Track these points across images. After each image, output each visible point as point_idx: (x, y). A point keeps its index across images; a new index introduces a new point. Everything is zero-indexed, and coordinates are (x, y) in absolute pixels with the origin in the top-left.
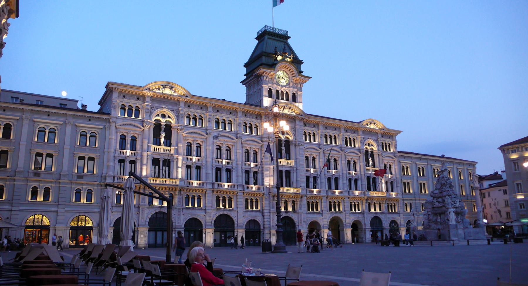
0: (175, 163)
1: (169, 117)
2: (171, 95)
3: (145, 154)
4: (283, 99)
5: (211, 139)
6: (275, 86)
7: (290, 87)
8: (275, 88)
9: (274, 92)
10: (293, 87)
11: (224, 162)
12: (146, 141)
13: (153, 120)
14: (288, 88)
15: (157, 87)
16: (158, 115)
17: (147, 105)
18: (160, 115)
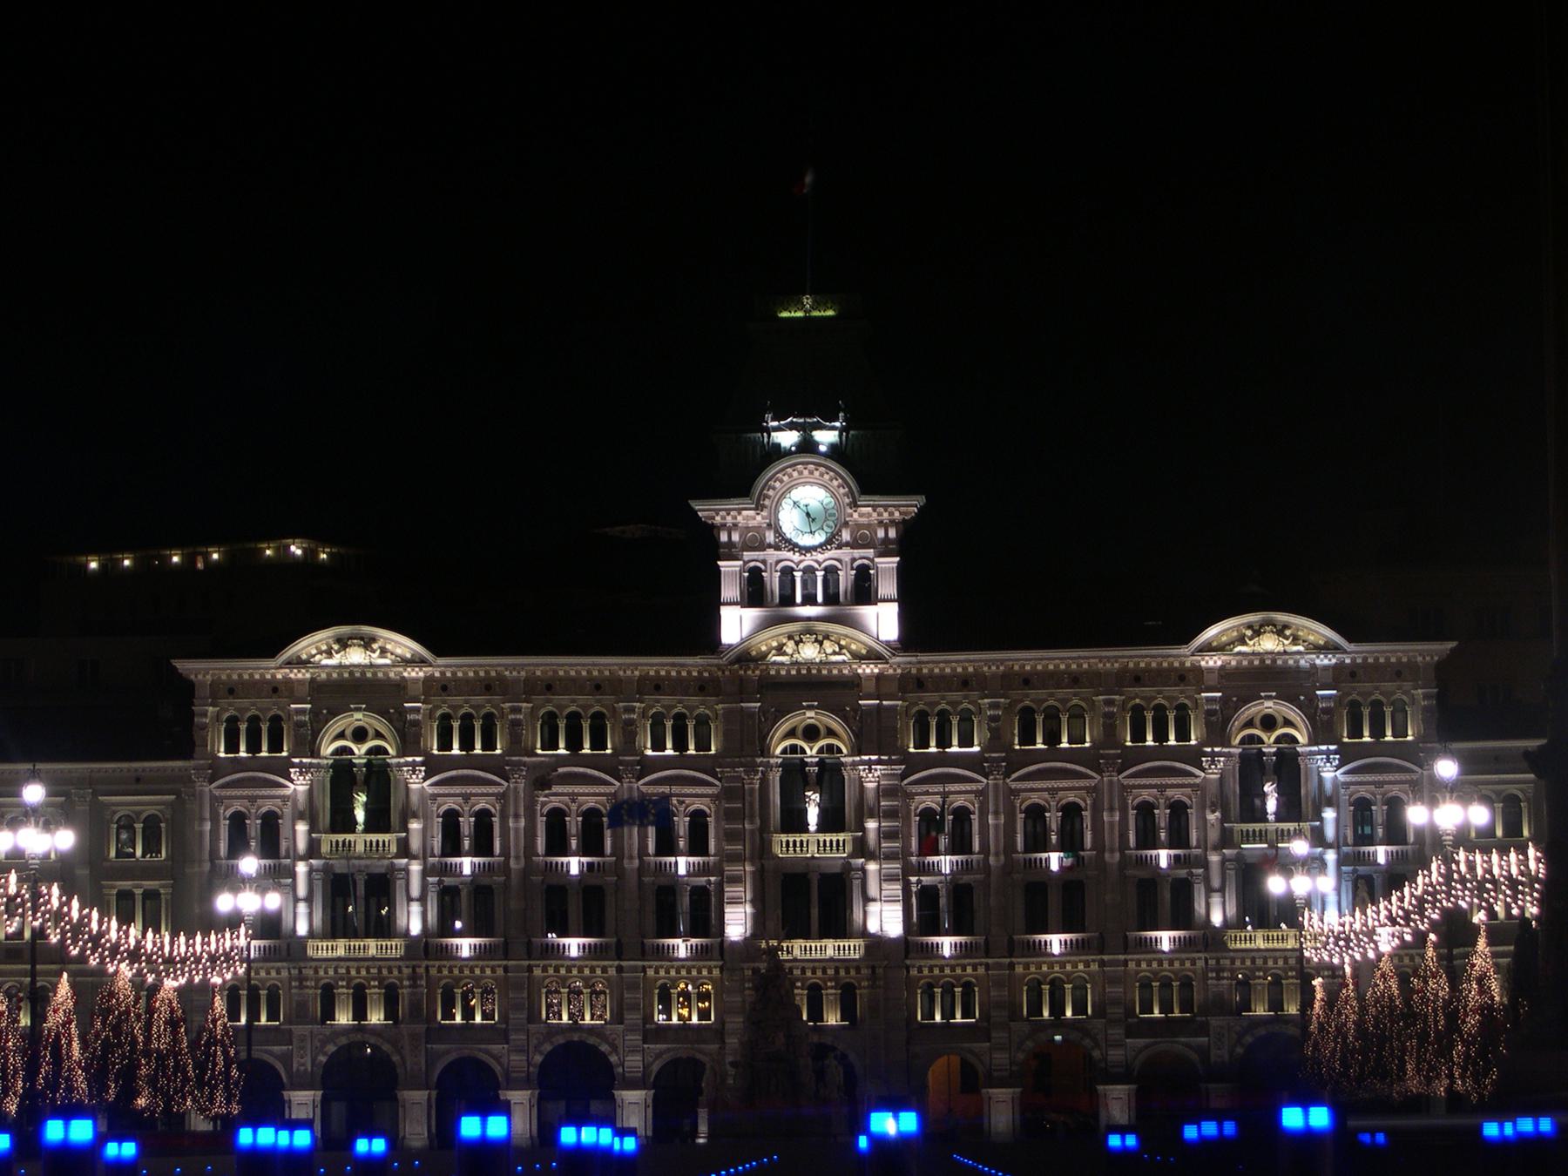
0: (400, 884)
1: (379, 735)
2: (372, 665)
4: (809, 600)
6: (771, 555)
7: (839, 547)
9: (773, 581)
10: (854, 544)
11: (1164, 857)
13: (778, 751)
14: (834, 553)
15: (324, 648)
16: (341, 736)
17: (1209, 700)
18: (1257, 721)
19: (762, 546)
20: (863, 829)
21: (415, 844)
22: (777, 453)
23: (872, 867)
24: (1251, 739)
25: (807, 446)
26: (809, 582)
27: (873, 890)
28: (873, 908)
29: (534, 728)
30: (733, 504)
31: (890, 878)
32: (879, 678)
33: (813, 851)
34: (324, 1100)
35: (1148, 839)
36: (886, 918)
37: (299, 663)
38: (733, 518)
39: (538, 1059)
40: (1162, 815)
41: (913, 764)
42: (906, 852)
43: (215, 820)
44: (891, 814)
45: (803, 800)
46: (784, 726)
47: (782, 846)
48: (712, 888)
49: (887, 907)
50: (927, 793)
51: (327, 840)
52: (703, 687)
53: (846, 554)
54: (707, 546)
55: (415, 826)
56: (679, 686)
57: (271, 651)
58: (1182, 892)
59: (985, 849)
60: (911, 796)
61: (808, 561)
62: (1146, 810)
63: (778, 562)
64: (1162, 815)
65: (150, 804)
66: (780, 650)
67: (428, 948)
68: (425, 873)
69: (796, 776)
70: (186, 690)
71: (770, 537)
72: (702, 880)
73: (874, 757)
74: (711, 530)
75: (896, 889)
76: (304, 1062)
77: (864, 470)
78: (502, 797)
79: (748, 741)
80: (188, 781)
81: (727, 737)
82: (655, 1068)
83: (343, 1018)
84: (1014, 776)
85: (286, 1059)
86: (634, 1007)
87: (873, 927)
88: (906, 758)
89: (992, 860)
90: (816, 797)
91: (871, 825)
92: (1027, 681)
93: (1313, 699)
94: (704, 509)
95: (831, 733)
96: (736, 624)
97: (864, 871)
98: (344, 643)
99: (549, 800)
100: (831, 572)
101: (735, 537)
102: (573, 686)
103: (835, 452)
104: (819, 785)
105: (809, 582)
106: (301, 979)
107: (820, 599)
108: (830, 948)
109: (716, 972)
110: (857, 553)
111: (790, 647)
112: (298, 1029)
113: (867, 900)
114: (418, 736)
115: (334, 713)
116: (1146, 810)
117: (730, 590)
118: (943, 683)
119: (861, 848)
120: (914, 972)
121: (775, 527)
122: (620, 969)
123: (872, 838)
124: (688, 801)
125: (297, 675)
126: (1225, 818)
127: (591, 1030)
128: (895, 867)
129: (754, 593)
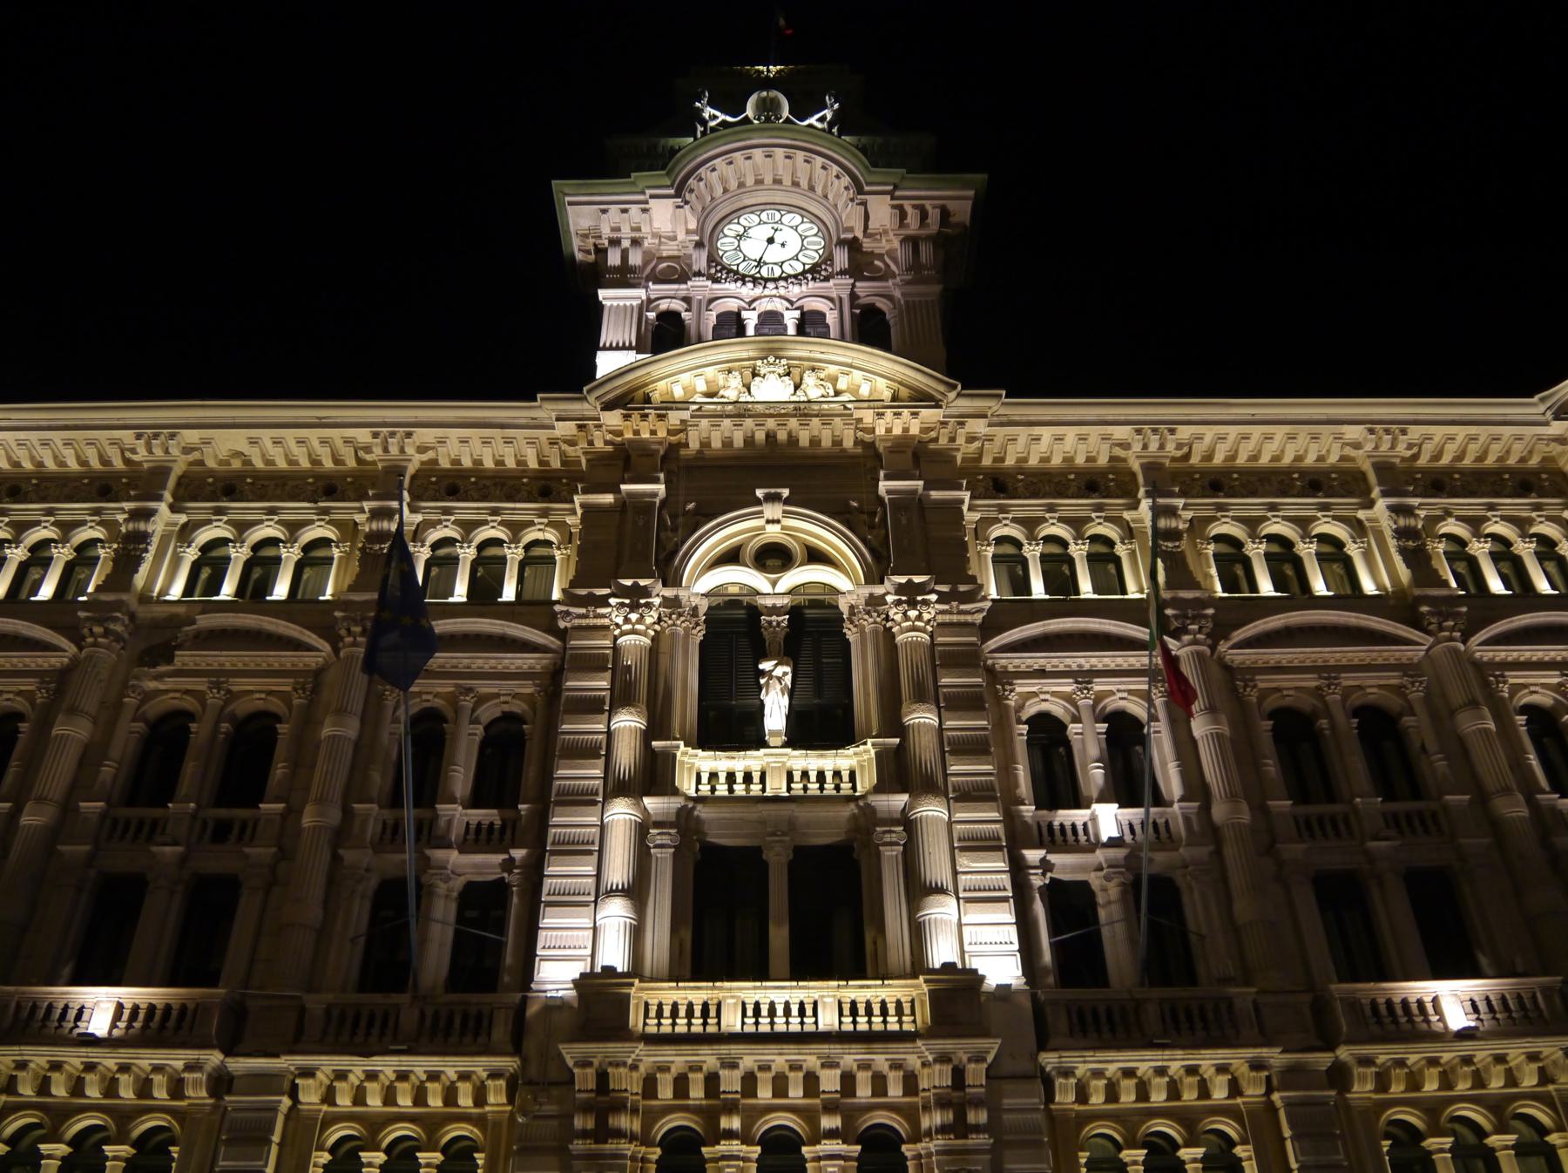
6: (700, 287)
20: (900, 730)
23: (932, 811)
27: (936, 867)
28: (941, 911)
29: (176, 562)
31: (978, 844)
36: (984, 941)
42: (1009, 805)
45: (754, 683)
48: (513, 878)
49: (974, 914)
50: (1042, 673)
59: (1196, 787)
63: (711, 301)
69: (734, 634)
71: (700, 261)
73: (917, 579)
75: (992, 869)
79: (632, 548)
84: (1240, 634)
89: (1219, 812)
90: (783, 671)
91: (922, 718)
92: (1219, 483)
97: (908, 823)
99: (166, 688)
101: (635, 259)
104: (789, 651)
108: (828, 1001)
109: (497, 1097)
110: (863, 288)
113: (919, 890)
119: (898, 771)
120: (1065, 1097)
122: (221, 1083)
123: (925, 749)
124: (485, 687)
128: (985, 818)
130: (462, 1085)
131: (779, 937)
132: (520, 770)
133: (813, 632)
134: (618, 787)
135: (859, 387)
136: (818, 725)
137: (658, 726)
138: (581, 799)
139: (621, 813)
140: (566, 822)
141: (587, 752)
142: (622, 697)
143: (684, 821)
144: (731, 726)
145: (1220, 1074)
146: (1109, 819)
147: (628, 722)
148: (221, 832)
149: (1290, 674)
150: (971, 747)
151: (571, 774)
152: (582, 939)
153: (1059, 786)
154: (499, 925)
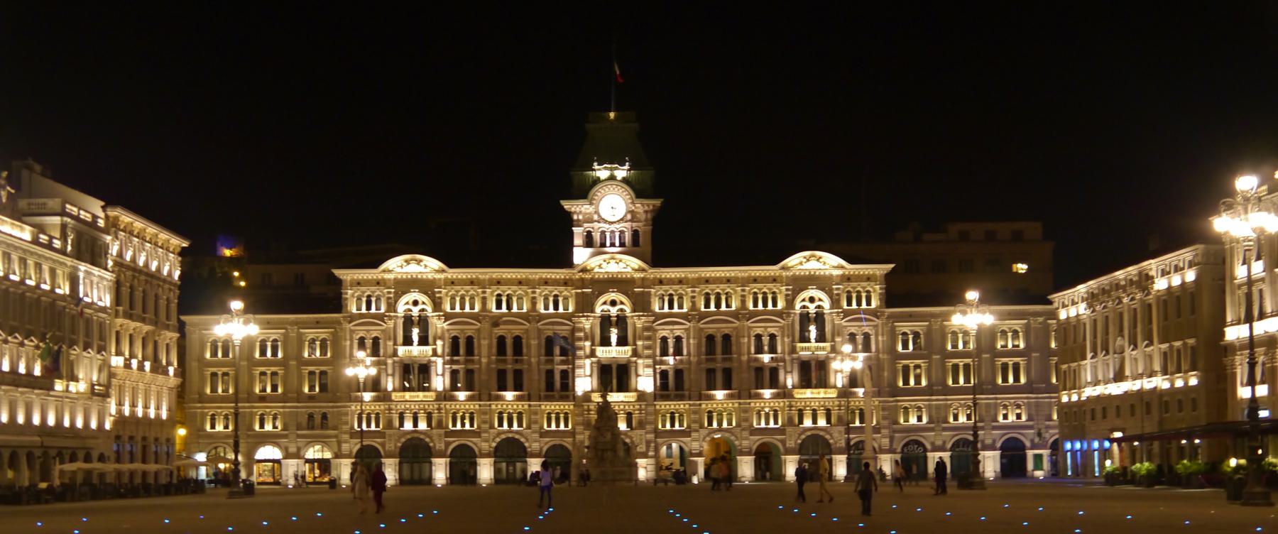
0: (433, 368)
3: (390, 361)
4: (613, 245)
5: (486, 325)
6: (596, 225)
8: (597, 228)
9: (597, 237)
12: (390, 343)
19: (592, 221)
21: (439, 351)
22: (597, 181)
23: (640, 361)
24: (804, 307)
25: (612, 178)
26: (612, 238)
27: (640, 371)
30: (581, 202)
31: (648, 366)
32: (643, 279)
33: (614, 355)
34: (400, 463)
35: (759, 350)
37: (390, 271)
38: (578, 208)
39: (494, 445)
40: (766, 340)
41: (658, 317)
43: (351, 340)
44: (649, 338)
46: (602, 300)
47: (602, 352)
51: (402, 350)
52: (566, 283)
53: (628, 225)
54: (567, 221)
55: (439, 343)
56: (556, 283)
57: (375, 265)
58: (774, 372)
59: (689, 354)
60: (656, 331)
61: (613, 227)
62: (758, 337)
64: (766, 340)
65: (323, 333)
66: (600, 266)
67: (445, 396)
68: (444, 364)
69: (606, 321)
70: (338, 282)
71: (596, 217)
72: (565, 367)
74: (568, 215)
75: (650, 371)
76: (390, 446)
77: (638, 189)
78: (478, 330)
79: (585, 305)
80: (340, 323)
81: (577, 304)
82: (545, 449)
83: (408, 426)
85: (383, 445)
86: (536, 422)
87: (640, 388)
88: (655, 314)
91: (640, 343)
93: (831, 290)
94: (567, 205)
95: (622, 303)
96: (581, 255)
98: (408, 262)
99: (499, 331)
100: (622, 232)
102: (509, 282)
103: (625, 180)
105: (612, 238)
106: (390, 409)
107: (617, 243)
111: (604, 265)
112: (388, 432)
113: (637, 375)
114: (441, 304)
115: (404, 293)
116: (758, 337)
117: (578, 240)
118: (671, 282)
121: (597, 212)
123: (640, 349)
125: (387, 276)
126: (793, 341)
127: (517, 432)
128: (650, 361)
129: (589, 242)
130: (568, 406)
131: (615, 381)
132: (569, 352)
133: (621, 321)
134: (587, 357)
135: (628, 265)
136: (622, 341)
137: (593, 344)
138: (580, 358)
139: (588, 362)
140: (578, 362)
141: (581, 349)
142: (586, 339)
143: (599, 362)
144: (605, 342)
145: (682, 406)
146: (671, 360)
147: (588, 344)
148: (517, 361)
149: (711, 329)
150: (648, 348)
151: (580, 353)
152: (584, 383)
153: (664, 352)
154: (567, 380)
